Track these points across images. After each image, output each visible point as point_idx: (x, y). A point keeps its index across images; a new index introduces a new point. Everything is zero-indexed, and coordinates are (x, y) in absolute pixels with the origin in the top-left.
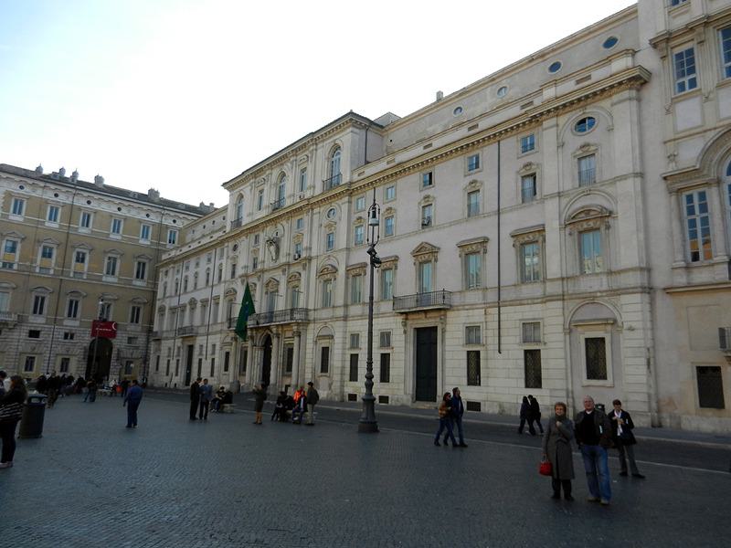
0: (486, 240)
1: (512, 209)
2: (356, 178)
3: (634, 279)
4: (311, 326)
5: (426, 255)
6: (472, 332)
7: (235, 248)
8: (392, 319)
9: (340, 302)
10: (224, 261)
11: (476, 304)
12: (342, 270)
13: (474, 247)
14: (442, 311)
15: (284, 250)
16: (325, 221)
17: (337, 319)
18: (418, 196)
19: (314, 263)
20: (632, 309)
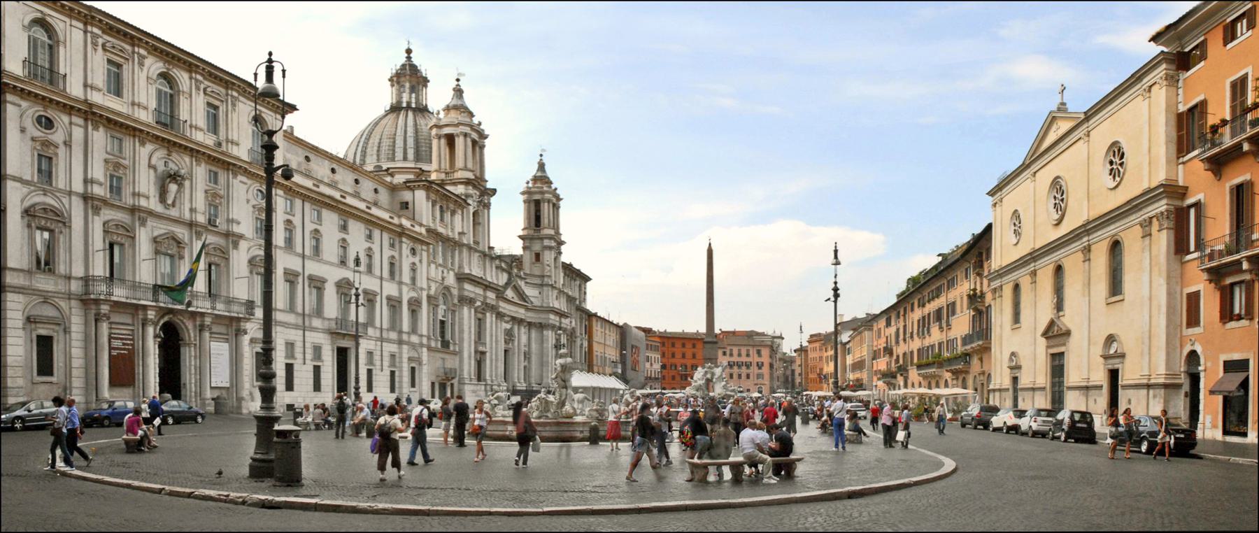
6: (370, 354)
8: (321, 335)
19: (243, 245)
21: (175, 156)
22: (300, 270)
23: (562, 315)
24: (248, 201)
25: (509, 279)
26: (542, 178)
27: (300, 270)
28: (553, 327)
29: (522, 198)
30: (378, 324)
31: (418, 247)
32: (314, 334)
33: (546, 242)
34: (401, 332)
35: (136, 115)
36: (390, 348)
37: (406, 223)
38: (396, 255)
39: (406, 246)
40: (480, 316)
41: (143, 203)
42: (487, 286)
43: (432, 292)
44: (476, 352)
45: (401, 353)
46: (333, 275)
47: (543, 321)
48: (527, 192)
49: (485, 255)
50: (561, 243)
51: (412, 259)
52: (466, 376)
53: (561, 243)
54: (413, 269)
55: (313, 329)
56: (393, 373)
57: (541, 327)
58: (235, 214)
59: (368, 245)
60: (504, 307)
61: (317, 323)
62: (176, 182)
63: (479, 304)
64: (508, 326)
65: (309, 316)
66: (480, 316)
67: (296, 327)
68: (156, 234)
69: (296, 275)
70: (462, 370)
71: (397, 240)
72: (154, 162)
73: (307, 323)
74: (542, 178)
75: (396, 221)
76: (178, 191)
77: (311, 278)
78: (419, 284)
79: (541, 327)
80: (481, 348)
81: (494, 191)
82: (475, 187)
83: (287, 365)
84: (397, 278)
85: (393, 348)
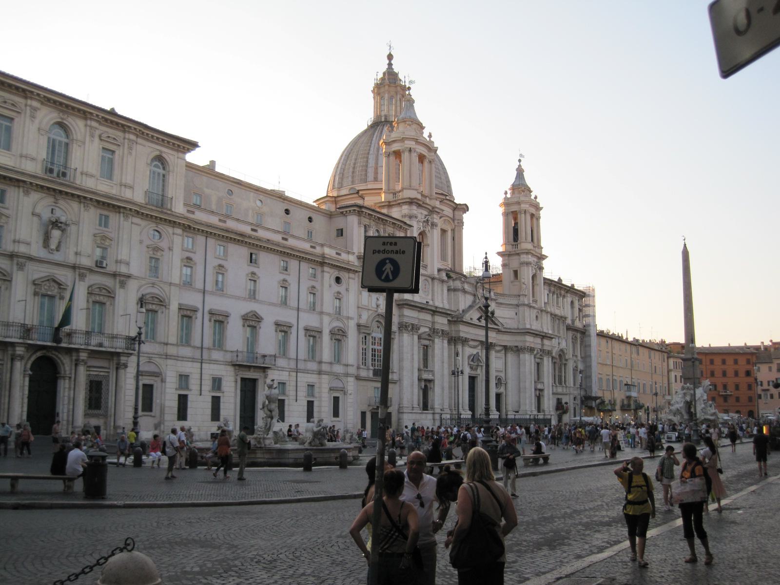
5: (252, 321)
8: (222, 367)
11: (286, 368)
12: (174, 307)
13: (285, 328)
14: (264, 369)
19: (133, 285)
20: (351, 384)
21: (62, 203)
22: (200, 306)
23: (544, 336)
24: (141, 242)
25: (474, 302)
26: (520, 186)
27: (200, 306)
28: (531, 350)
29: (501, 210)
30: (292, 354)
31: (344, 275)
32: (212, 366)
33: (524, 258)
34: (320, 362)
35: (23, 167)
36: (304, 379)
37: (327, 251)
38: (317, 285)
39: (329, 275)
40: (426, 342)
41: (22, 249)
42: (435, 312)
43: (363, 321)
44: (420, 380)
45: (320, 383)
46: (237, 309)
47: (520, 345)
48: (507, 203)
49: (433, 279)
50: (542, 257)
51: (336, 288)
52: (406, 403)
53: (542, 257)
54: (338, 297)
55: (211, 361)
56: (310, 404)
57: (518, 350)
58: (123, 255)
59: (282, 277)
60: (465, 331)
61: (217, 355)
62: (59, 228)
63: (423, 330)
64: (474, 351)
65: (209, 349)
66: (426, 342)
67: (193, 360)
68: (36, 276)
69: (195, 311)
70: (401, 399)
71: (319, 269)
72: (37, 211)
73: (205, 356)
74: (520, 186)
75: (318, 250)
76: (62, 236)
77: (211, 313)
78: (344, 313)
79: (518, 350)
80: (425, 376)
81: (465, 208)
82: (419, 206)
83: (180, 396)
84: (318, 309)
85: (312, 379)
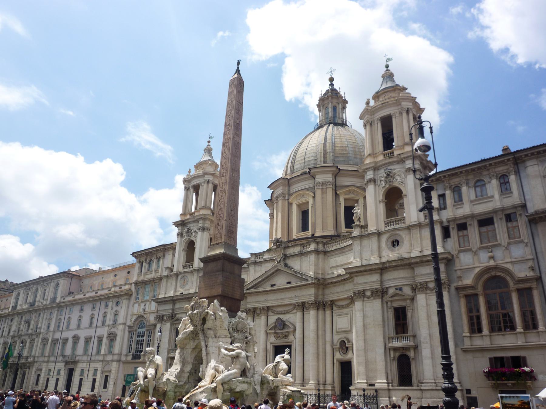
0: (91, 338)
1: (100, 327)
2: (62, 300)
3: (116, 357)
4: (35, 364)
5: (76, 339)
6: (83, 370)
7: (12, 320)
9: (47, 354)
10: (5, 326)
12: (50, 341)
15: (31, 327)
16: (48, 317)
17: (44, 362)
18: (78, 314)
59: (92, 312)
